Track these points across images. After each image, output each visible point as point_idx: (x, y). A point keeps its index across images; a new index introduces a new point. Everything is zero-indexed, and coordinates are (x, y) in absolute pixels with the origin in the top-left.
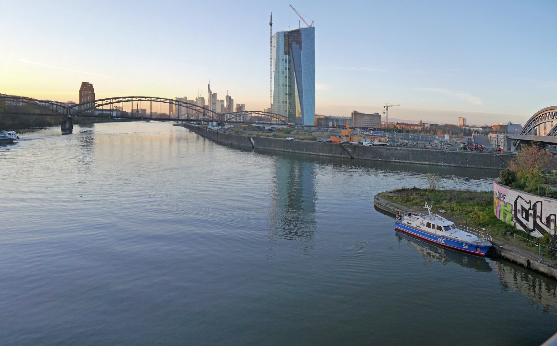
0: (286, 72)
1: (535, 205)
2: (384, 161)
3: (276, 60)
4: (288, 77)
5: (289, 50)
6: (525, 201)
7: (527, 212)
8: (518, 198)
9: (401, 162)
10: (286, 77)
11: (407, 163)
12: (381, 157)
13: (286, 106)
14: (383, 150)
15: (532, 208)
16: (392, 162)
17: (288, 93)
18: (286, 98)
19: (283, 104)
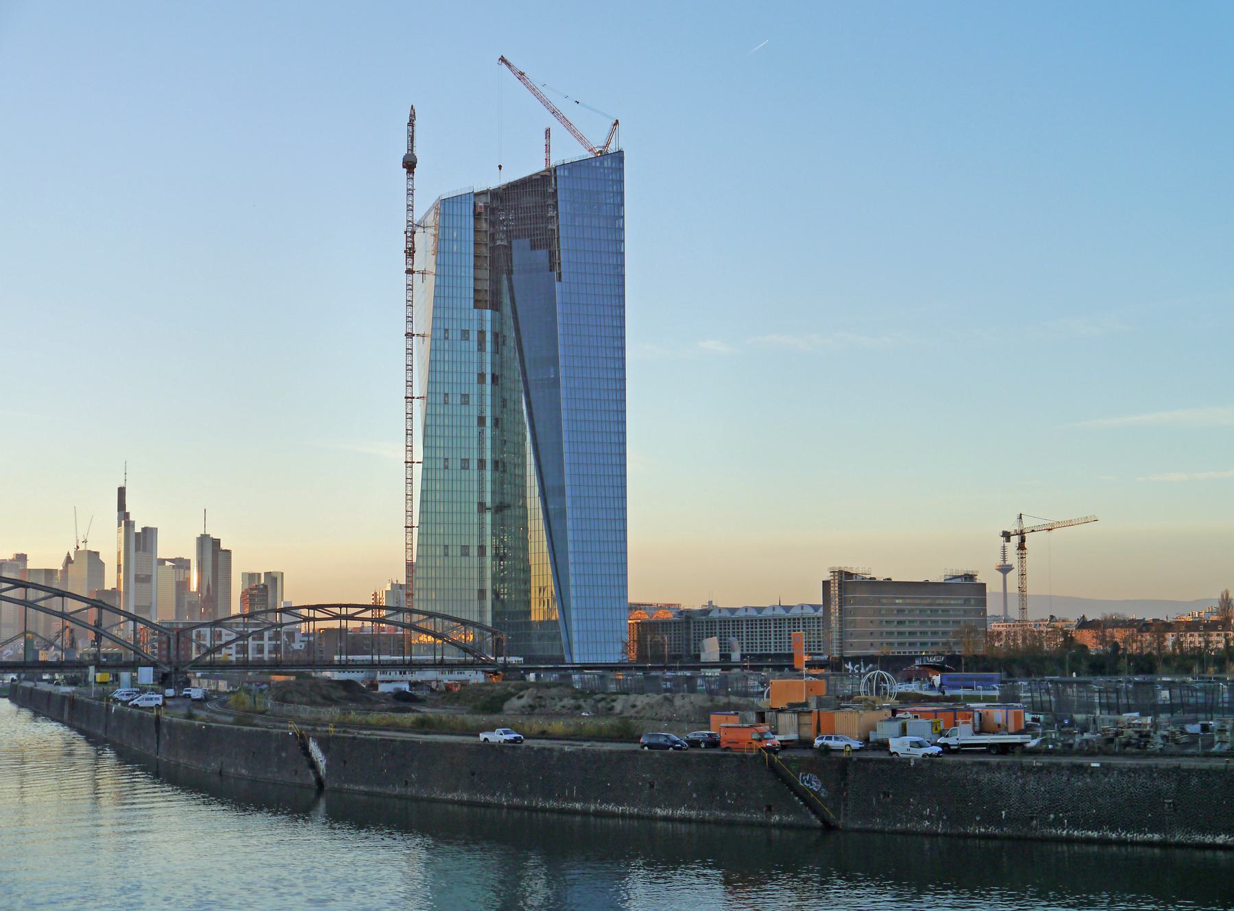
0: (481, 395)
2: (1010, 838)
3: (434, 340)
4: (488, 422)
5: (495, 282)
9: (1109, 842)
10: (481, 421)
11: (1151, 844)
12: (991, 818)
13: (482, 569)
14: (1001, 776)
16: (1059, 840)
17: (489, 504)
18: (481, 525)
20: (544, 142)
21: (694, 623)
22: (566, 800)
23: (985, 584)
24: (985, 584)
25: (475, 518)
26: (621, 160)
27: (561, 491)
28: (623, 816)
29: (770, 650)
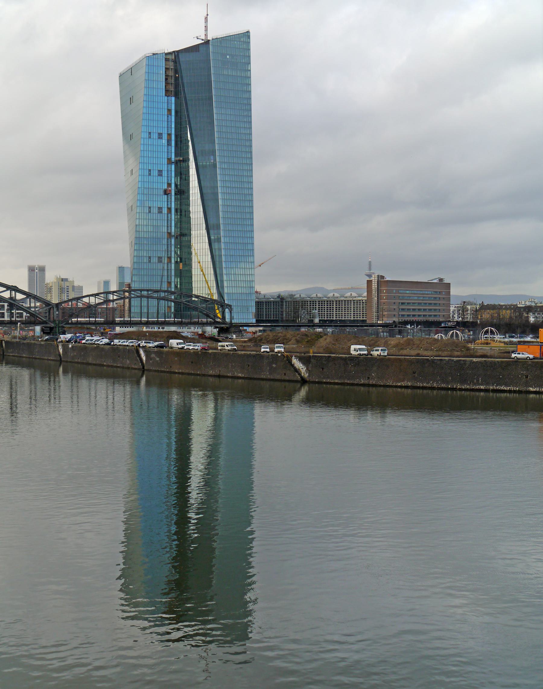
19: (160, 266)
20: (203, 24)
21: (286, 302)
22: (475, 384)
23: (449, 284)
24: (449, 284)
25: (165, 241)
26: (249, 37)
27: (218, 227)
28: (510, 391)
29: (333, 318)
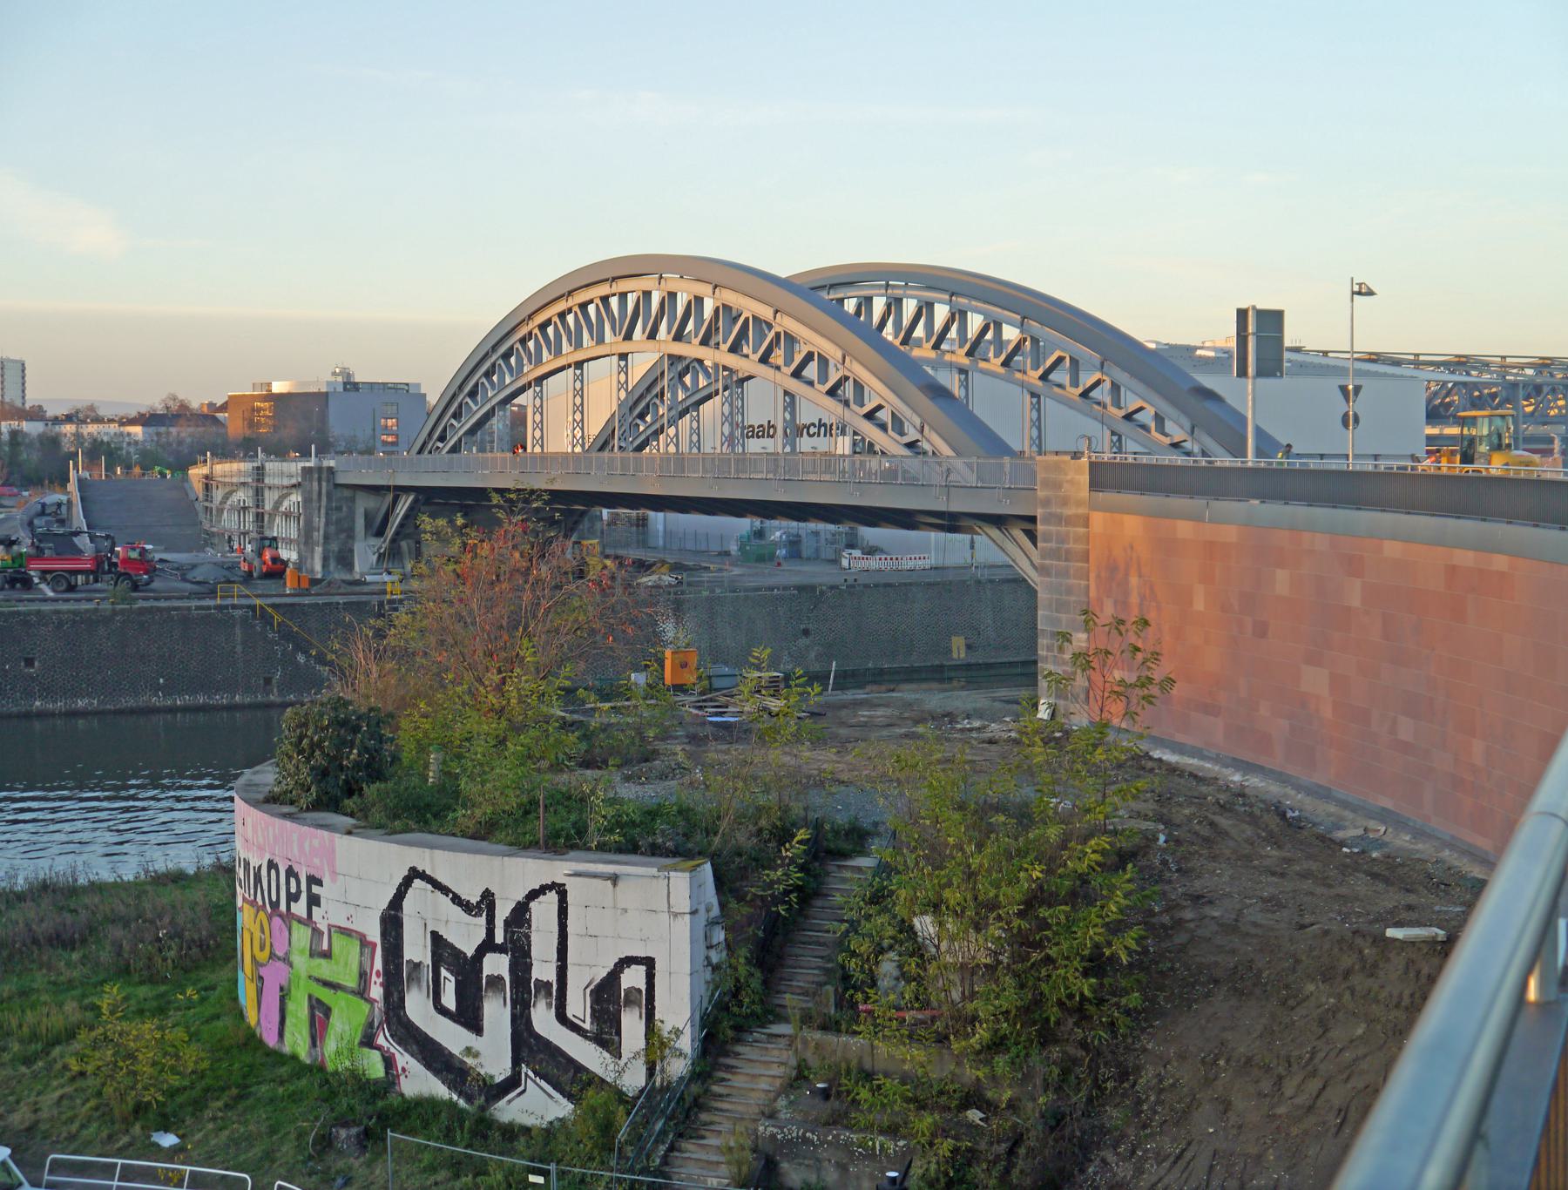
1: (520, 915)
6: (457, 900)
7: (468, 970)
8: (407, 883)
15: (499, 938)
